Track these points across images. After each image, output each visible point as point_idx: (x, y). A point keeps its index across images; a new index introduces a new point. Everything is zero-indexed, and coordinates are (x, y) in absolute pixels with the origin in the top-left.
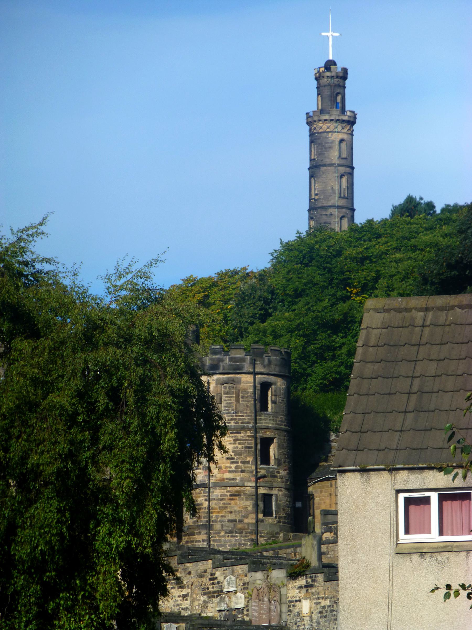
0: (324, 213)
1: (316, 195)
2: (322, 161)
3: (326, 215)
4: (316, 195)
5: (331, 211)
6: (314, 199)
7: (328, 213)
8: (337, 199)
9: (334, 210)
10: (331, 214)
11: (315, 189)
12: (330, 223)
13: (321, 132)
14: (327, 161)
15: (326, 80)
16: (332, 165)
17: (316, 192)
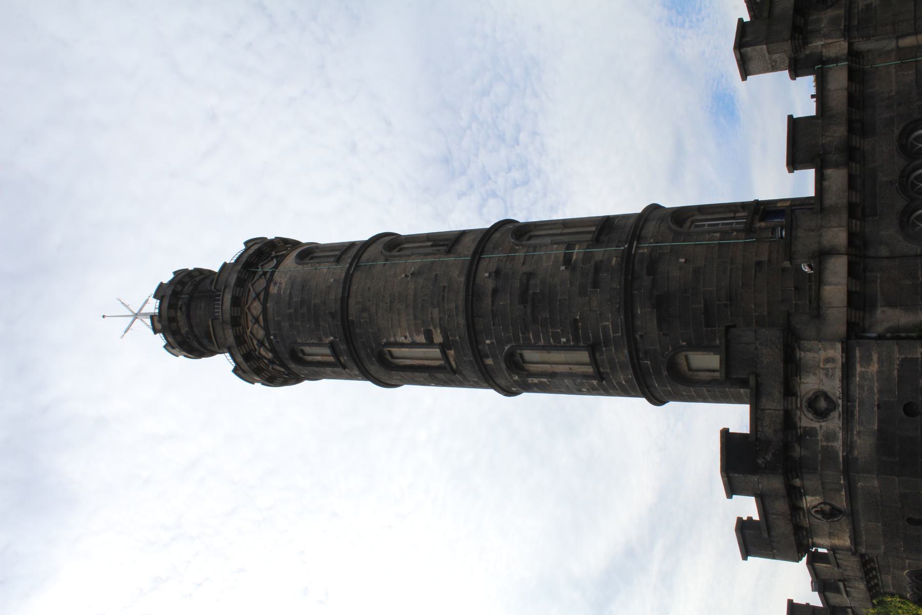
0: (488, 300)
1: (429, 335)
2: (333, 315)
3: (495, 292)
4: (429, 335)
5: (484, 274)
6: (444, 347)
7: (490, 285)
8: (451, 259)
9: (483, 264)
10: (497, 273)
11: (414, 345)
12: (530, 275)
13: (266, 320)
14: (336, 293)
15: (179, 314)
16: (348, 279)
17: (421, 339)
